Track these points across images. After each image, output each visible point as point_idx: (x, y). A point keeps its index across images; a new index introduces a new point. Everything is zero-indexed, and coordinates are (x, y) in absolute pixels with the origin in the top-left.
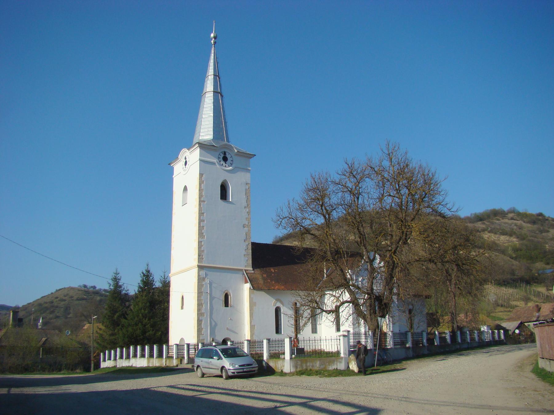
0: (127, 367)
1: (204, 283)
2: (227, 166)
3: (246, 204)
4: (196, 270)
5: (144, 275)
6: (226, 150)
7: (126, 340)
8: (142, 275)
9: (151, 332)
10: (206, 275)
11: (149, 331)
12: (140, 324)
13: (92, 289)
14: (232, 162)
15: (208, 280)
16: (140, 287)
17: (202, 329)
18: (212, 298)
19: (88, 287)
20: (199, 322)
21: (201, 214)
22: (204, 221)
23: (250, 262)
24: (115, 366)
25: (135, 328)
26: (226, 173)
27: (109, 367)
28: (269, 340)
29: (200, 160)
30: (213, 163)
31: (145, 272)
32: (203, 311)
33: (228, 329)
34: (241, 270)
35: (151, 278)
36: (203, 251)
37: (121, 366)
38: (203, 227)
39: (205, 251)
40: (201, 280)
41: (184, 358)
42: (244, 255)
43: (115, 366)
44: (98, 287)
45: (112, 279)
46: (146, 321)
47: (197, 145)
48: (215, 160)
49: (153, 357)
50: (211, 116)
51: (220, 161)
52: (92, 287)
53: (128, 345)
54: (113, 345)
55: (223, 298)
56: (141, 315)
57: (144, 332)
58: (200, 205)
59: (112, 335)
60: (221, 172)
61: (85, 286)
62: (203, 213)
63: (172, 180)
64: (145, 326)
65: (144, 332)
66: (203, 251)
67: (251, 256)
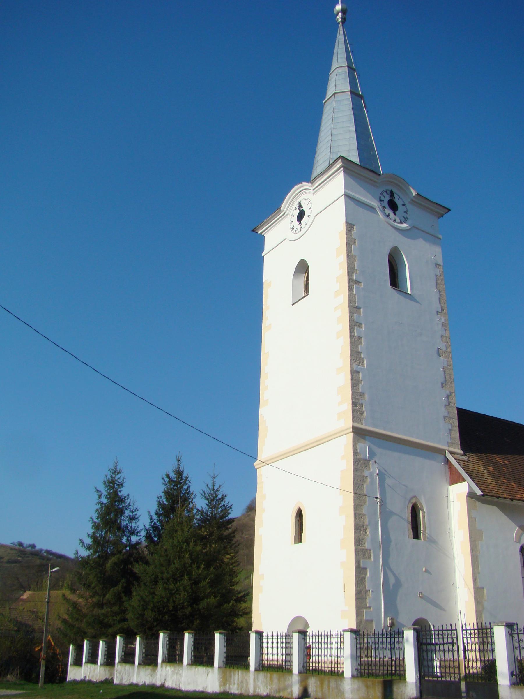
0: (144, 685)
1: (366, 473)
2: (398, 220)
3: (439, 306)
4: (347, 440)
5: (171, 481)
6: (394, 190)
7: (149, 615)
8: (167, 479)
9: (212, 600)
10: (372, 454)
11: (207, 597)
12: (186, 577)
13: (30, 548)
14: (405, 215)
15: (376, 466)
16: (160, 503)
17: (367, 592)
18: (386, 515)
19: (25, 546)
20: (360, 572)
21: (354, 309)
22: (359, 325)
23: (456, 435)
24: (108, 682)
25: (172, 586)
26: (397, 233)
27: (90, 682)
28: (510, 626)
29: (346, 195)
30: (372, 209)
31: (172, 475)
32: (367, 545)
33: (423, 597)
34: (441, 452)
35: (185, 487)
36: (362, 394)
37: (126, 682)
38: (360, 338)
39: (366, 397)
40: (360, 464)
41: (402, 676)
42: (445, 417)
43: (108, 682)
44: (38, 547)
45: (105, 483)
46: (198, 571)
47: (339, 164)
48: (375, 204)
49: (210, 662)
50: (350, 131)
51: (384, 208)
52: (30, 546)
53: (151, 629)
54: (103, 629)
55: (408, 516)
56: (187, 555)
57: (195, 600)
58: (350, 288)
59: (100, 605)
60: (387, 232)
61: (21, 544)
62: (359, 308)
63: (261, 260)
64: (196, 582)
65: (195, 600)
66: (362, 394)
67: (456, 423)
